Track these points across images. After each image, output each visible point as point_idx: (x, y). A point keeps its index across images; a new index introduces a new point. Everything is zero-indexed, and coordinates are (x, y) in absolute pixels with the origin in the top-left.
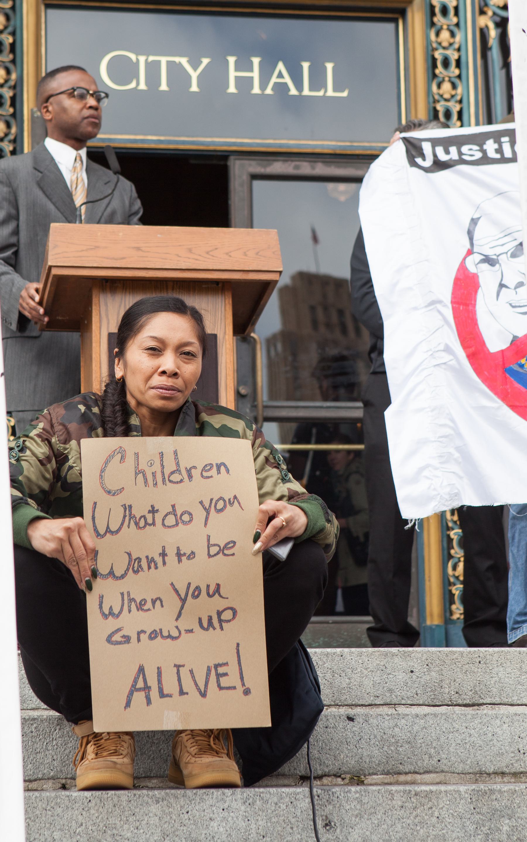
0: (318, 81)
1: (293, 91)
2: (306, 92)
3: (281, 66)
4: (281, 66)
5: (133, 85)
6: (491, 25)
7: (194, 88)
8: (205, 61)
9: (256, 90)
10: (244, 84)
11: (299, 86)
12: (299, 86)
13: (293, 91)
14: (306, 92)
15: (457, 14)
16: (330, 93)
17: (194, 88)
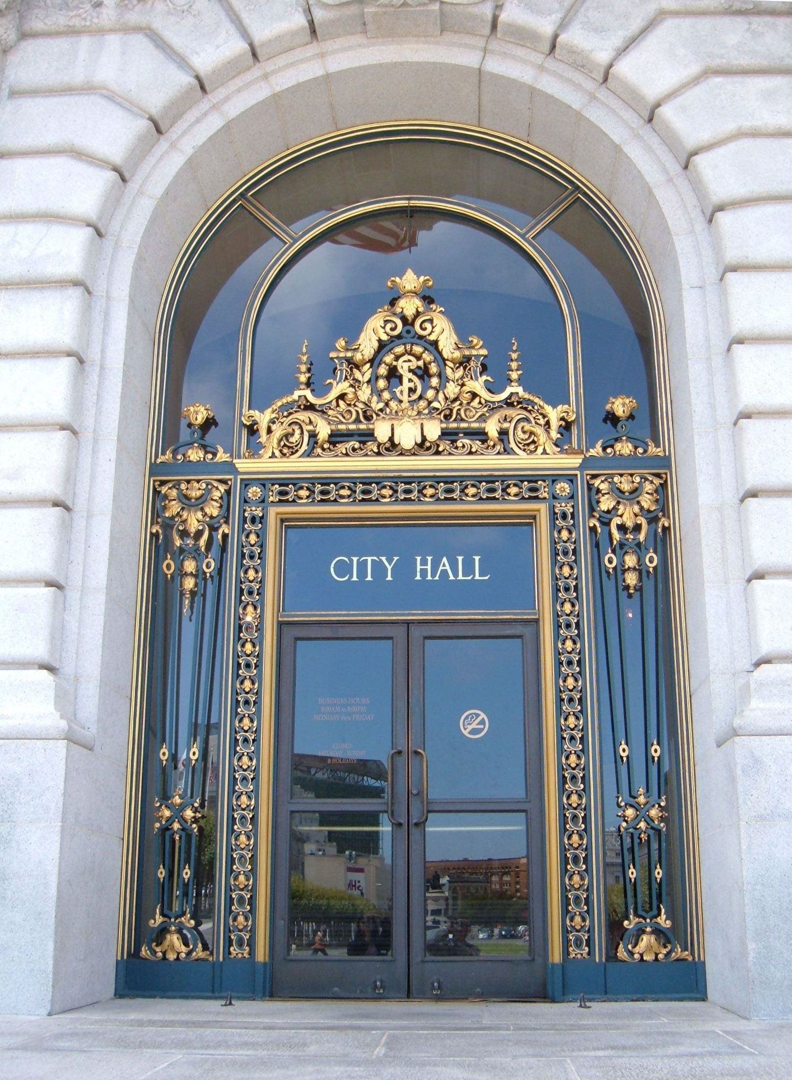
0: (469, 568)
1: (452, 578)
2: (460, 577)
3: (445, 560)
4: (445, 560)
5: (346, 578)
6: (598, 524)
7: (389, 578)
8: (396, 558)
9: (429, 578)
10: (424, 572)
11: (456, 574)
12: (456, 574)
13: (452, 578)
14: (460, 577)
15: (573, 517)
16: (477, 577)
17: (389, 578)
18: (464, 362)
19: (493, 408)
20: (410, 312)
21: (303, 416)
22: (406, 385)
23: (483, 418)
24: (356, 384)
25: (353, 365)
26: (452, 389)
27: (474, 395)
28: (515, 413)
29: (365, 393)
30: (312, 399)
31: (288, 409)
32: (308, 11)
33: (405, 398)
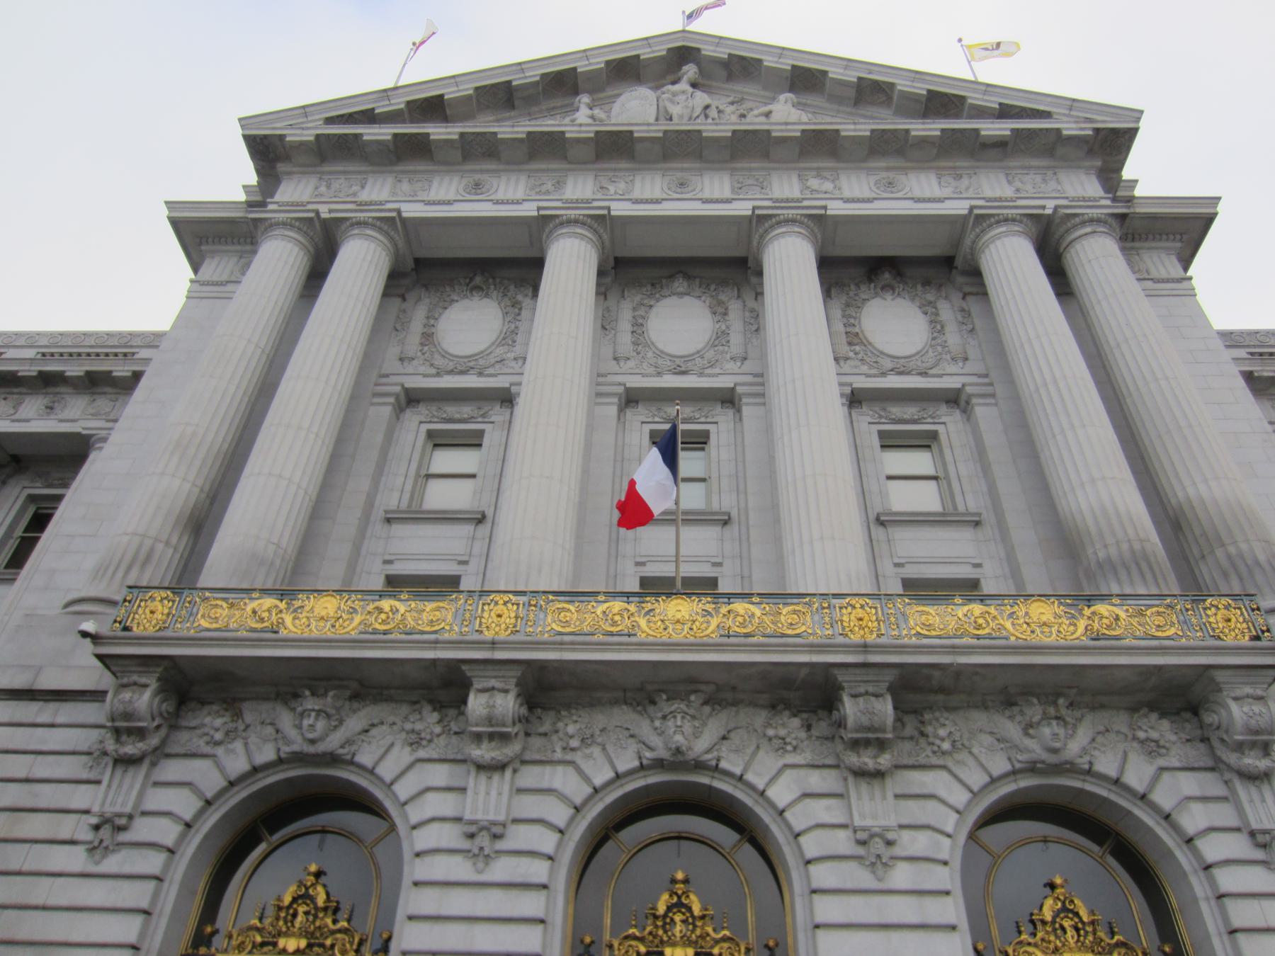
18: (703, 917)
19: (717, 942)
20: (680, 892)
21: (633, 943)
22: (678, 928)
23: (712, 947)
24: (656, 927)
25: (656, 917)
26: (698, 932)
27: (708, 935)
28: (726, 945)
29: (660, 932)
30: (638, 934)
31: (627, 938)
32: (640, 758)
33: (678, 935)
